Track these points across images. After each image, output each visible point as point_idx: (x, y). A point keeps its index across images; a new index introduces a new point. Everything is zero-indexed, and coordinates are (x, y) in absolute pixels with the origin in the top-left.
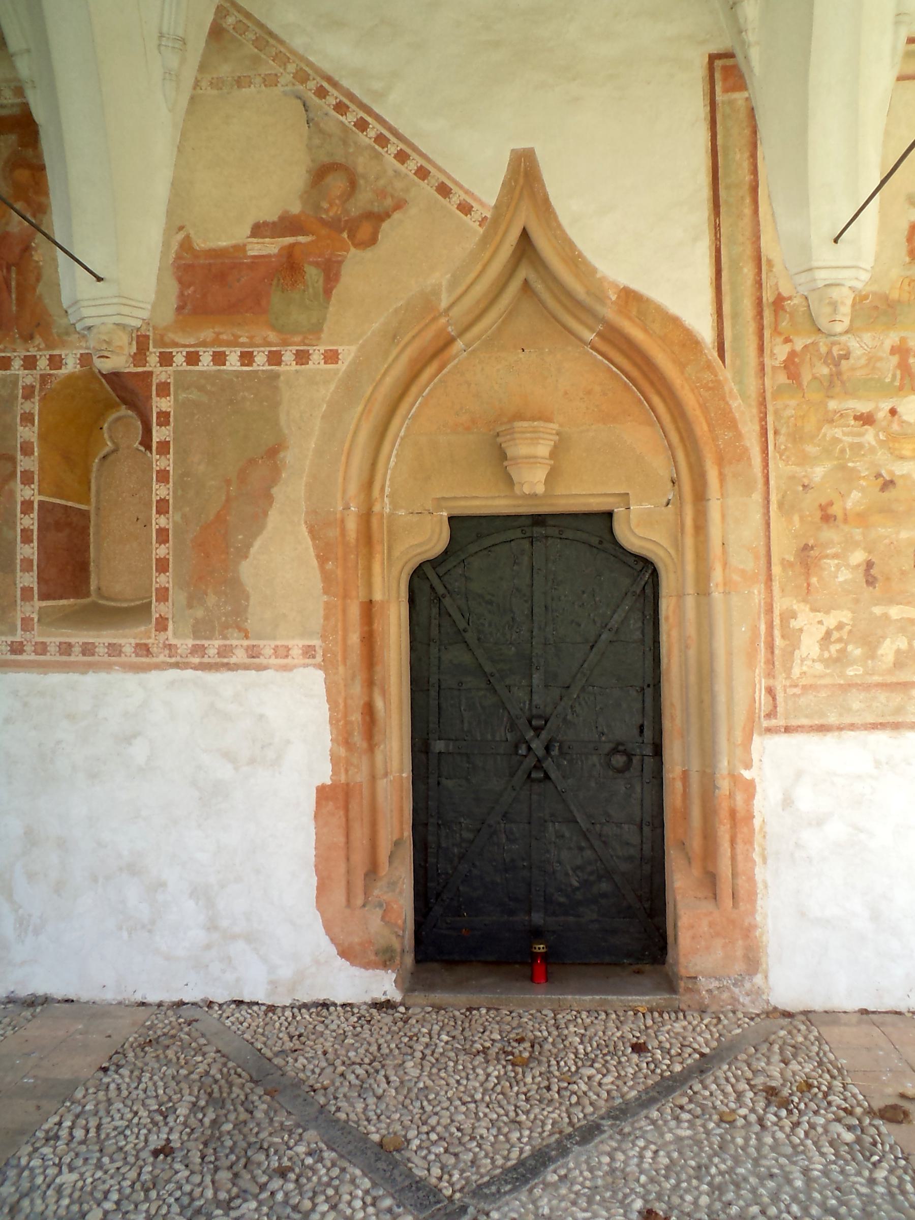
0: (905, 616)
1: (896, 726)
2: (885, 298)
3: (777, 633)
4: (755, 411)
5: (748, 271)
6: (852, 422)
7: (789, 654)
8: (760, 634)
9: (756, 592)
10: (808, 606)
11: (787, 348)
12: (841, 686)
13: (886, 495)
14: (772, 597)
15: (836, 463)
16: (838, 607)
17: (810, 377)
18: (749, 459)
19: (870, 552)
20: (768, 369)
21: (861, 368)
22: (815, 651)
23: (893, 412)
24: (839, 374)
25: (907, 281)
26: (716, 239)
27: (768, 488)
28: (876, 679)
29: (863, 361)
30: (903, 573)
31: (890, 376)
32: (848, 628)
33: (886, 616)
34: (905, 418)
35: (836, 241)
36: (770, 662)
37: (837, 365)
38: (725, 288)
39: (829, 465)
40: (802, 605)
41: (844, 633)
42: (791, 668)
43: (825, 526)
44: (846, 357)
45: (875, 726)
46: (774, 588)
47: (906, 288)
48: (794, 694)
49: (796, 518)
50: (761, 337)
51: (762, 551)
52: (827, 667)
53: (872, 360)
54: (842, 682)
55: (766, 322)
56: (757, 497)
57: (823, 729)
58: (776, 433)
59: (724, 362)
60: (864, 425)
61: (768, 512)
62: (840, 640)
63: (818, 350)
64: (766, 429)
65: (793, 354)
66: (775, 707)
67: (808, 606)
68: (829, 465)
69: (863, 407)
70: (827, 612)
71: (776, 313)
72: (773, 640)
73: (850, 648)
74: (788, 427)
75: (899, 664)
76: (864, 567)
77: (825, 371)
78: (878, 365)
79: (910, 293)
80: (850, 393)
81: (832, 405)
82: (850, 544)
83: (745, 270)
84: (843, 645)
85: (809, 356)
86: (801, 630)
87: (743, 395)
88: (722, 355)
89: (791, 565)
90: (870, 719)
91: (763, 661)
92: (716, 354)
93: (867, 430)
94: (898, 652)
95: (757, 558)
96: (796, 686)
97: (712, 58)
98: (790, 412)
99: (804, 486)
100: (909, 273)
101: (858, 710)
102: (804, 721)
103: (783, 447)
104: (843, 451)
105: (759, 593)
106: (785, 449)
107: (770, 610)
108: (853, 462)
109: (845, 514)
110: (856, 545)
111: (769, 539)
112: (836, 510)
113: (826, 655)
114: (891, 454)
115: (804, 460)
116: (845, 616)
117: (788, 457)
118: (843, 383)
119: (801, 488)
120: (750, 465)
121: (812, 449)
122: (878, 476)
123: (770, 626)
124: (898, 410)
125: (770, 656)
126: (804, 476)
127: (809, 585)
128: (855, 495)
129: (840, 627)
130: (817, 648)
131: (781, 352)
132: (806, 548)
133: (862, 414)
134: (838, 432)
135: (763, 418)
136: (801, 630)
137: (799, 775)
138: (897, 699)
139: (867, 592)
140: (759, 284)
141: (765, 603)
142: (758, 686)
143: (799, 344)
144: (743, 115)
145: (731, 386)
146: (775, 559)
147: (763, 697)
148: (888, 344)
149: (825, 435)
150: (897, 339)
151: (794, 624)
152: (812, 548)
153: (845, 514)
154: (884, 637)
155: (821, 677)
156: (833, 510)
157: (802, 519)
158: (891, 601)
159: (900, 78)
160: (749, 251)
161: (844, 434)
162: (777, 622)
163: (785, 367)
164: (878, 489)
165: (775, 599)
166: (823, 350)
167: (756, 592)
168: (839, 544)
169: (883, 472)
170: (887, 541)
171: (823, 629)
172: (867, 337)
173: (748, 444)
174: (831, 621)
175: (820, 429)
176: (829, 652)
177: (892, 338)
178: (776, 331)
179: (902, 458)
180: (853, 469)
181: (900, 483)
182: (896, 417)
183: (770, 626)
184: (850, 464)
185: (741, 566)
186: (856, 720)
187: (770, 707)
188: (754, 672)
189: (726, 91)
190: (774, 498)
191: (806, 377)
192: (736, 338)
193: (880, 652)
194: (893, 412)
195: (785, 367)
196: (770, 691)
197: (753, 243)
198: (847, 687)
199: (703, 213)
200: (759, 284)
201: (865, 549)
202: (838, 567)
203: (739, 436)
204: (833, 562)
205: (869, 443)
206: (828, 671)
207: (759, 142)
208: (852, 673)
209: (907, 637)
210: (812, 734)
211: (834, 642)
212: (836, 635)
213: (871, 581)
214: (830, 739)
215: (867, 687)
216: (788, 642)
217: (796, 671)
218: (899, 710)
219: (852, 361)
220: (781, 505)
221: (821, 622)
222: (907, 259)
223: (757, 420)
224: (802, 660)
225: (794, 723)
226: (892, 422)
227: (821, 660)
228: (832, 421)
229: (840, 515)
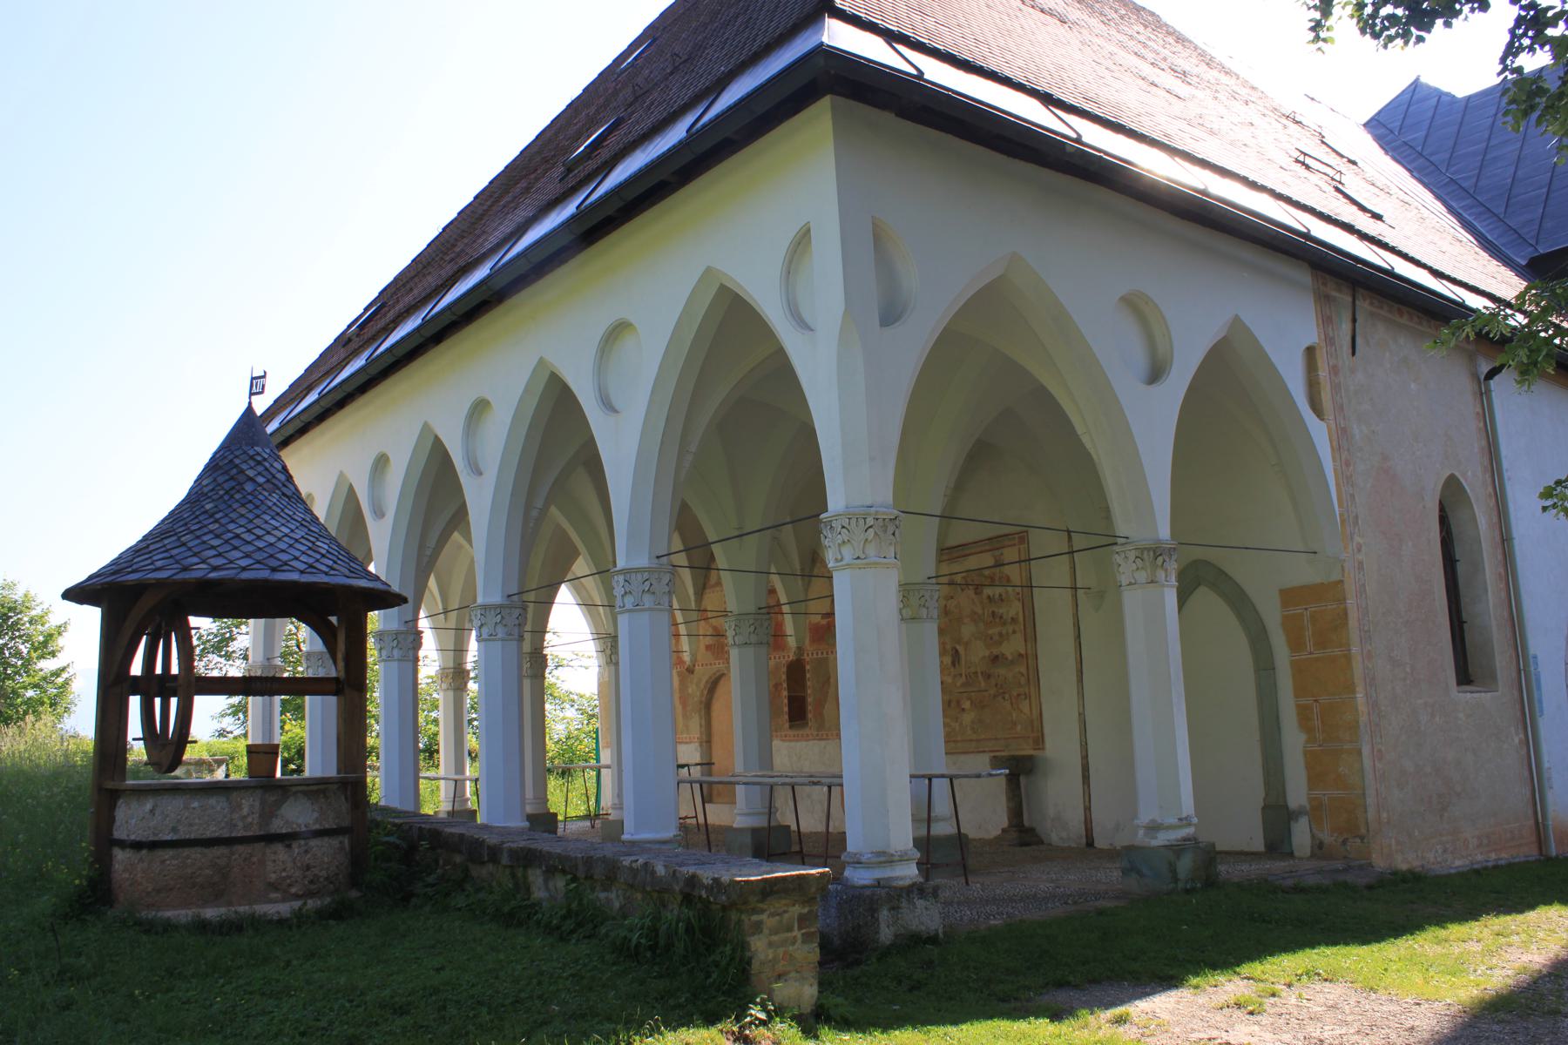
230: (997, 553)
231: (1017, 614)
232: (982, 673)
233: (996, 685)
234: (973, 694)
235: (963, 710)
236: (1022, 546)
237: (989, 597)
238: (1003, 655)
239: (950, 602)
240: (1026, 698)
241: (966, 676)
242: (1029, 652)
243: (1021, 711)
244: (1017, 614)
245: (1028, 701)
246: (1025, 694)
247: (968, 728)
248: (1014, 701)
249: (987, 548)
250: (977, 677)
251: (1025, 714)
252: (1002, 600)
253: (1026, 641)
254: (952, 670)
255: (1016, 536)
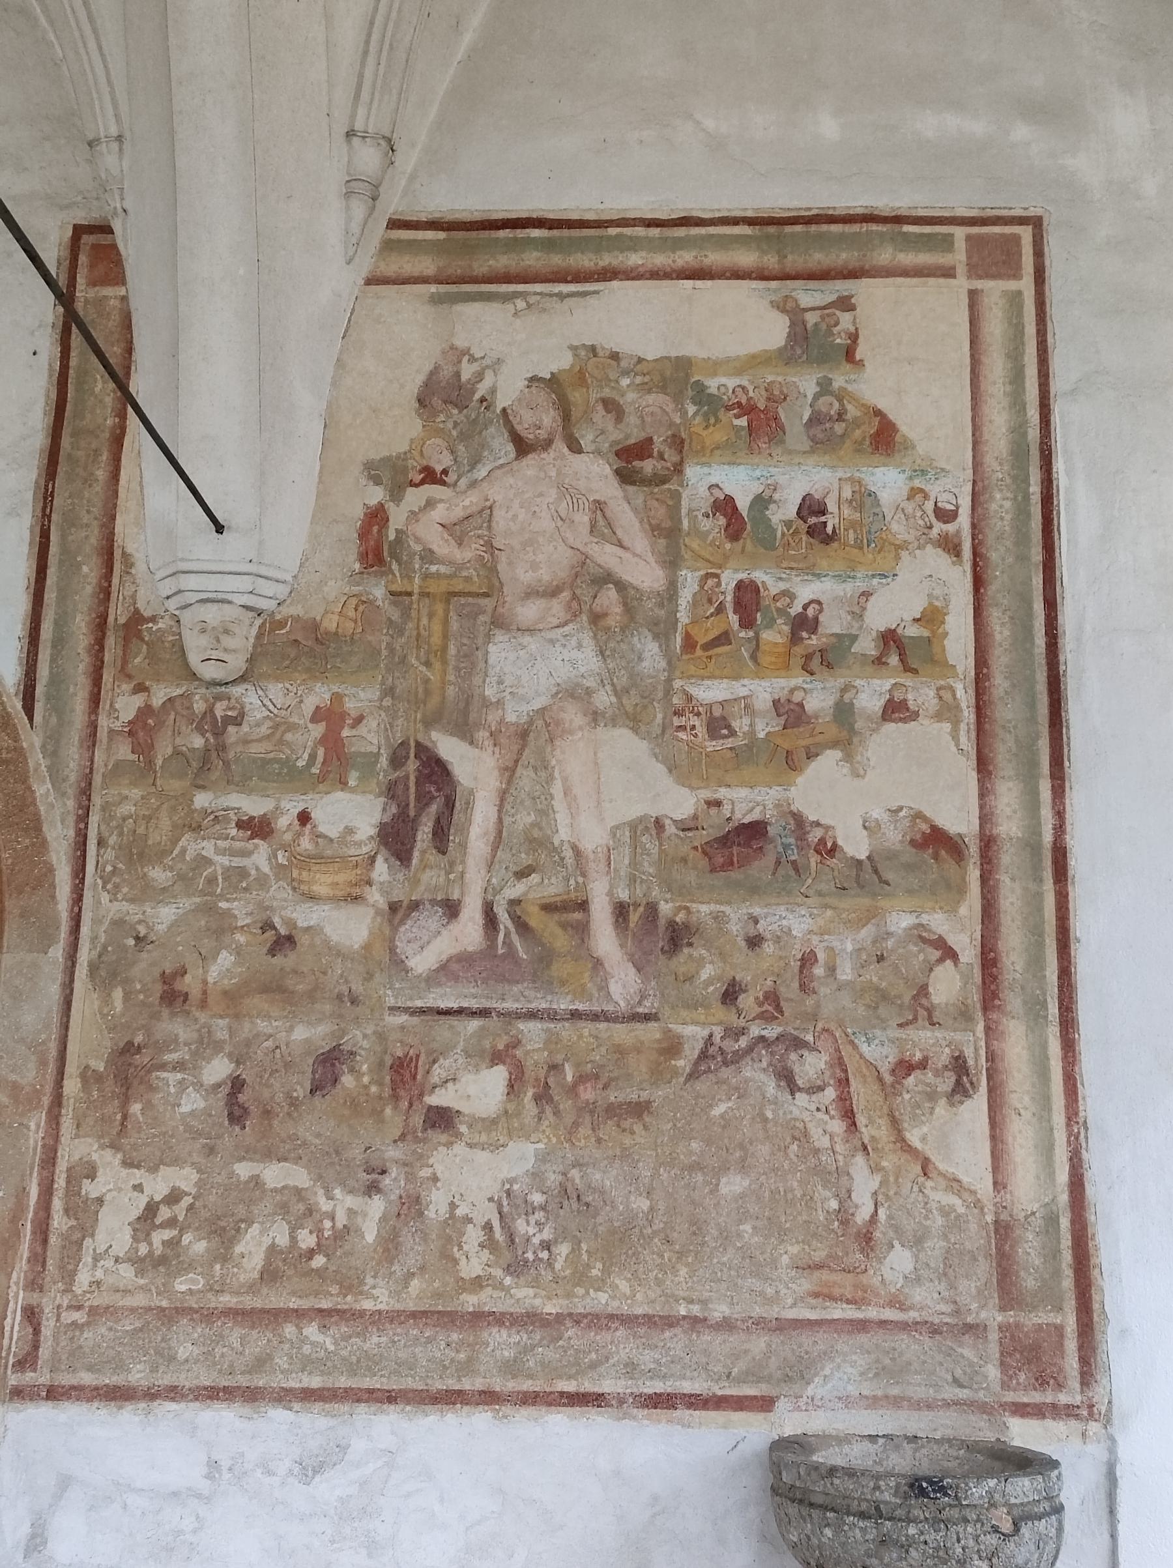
0: (291, 1183)
1: (252, 1396)
2: (313, 627)
3: (57, 1204)
4: (71, 804)
5: (90, 571)
6: (234, 832)
7: (74, 1246)
8: (28, 1205)
9: (33, 1126)
10: (119, 1156)
11: (138, 701)
12: (163, 1310)
13: (278, 960)
14: (57, 1139)
15: (198, 900)
16: (176, 1162)
17: (169, 751)
18: (53, 886)
19: (238, 1063)
20: (102, 734)
21: (259, 740)
22: (122, 1241)
23: (304, 817)
24: (222, 748)
25: (354, 601)
26: (44, 515)
27: (77, 939)
28: (227, 1300)
29: (264, 730)
30: (294, 1103)
31: (306, 756)
32: (187, 1201)
33: (256, 1181)
34: (322, 829)
35: (219, 529)
36: (38, 1259)
37: (219, 733)
38: (50, 596)
39: (187, 903)
40: (108, 1153)
41: (180, 1209)
42: (74, 1272)
43: (165, 1012)
44: (238, 721)
45: (212, 1394)
46: (63, 1119)
47: (351, 613)
48: (74, 1323)
49: (118, 994)
50: (97, 682)
51: (53, 1053)
52: (140, 1273)
53: (280, 726)
54: (165, 1304)
55: (107, 657)
56: (58, 952)
57: (118, 1395)
58: (101, 843)
59: (31, 718)
60: (252, 838)
61: (72, 981)
62: (171, 1223)
63: (190, 708)
64: (85, 836)
65: (146, 711)
66: (36, 1346)
67: (119, 1156)
68: (187, 903)
69: (253, 806)
70: (153, 1170)
71: (126, 641)
72: (48, 1216)
73: (187, 1239)
74: (121, 834)
75: (269, 1275)
76: (224, 1090)
77: (198, 742)
78: (289, 737)
79: (355, 622)
80: (242, 784)
81: (202, 800)
82: (206, 1045)
83: (85, 569)
84: (175, 1232)
85: (172, 717)
86: (100, 1201)
87: (55, 773)
88: (29, 709)
89: (99, 1078)
90: (206, 1379)
91: (26, 1255)
92: (19, 705)
93: (256, 846)
94: (272, 1249)
95: (43, 1063)
96: (79, 1308)
97: (79, 231)
98: (127, 809)
99: (138, 939)
100: (356, 589)
101: (187, 1361)
102: (87, 1378)
103: (109, 868)
104: (212, 880)
105: (38, 1126)
106: (113, 872)
107: (50, 1159)
108: (227, 900)
109: (205, 992)
110: (218, 1047)
111: (67, 1028)
112: (190, 983)
113: (143, 1249)
114: (294, 889)
115: (147, 893)
116: (185, 1178)
117: (117, 886)
118: (226, 764)
119: (132, 942)
120: (53, 897)
121: (159, 875)
122: (267, 926)
123: (47, 1191)
124: (313, 815)
125: (39, 1250)
126: (140, 922)
127: (125, 1117)
128: (225, 959)
129: (173, 1197)
130: (126, 1235)
131: (127, 706)
132: (130, 1049)
133: (252, 818)
134: (208, 848)
135: (83, 818)
136: (100, 1201)
137: (65, 1483)
138: (258, 1341)
139: (230, 1138)
140: (105, 593)
141: (44, 1146)
142: (11, 1305)
143: (160, 695)
144: (115, 319)
145: (37, 760)
146: (71, 1069)
147: (16, 1328)
148: (309, 707)
149: (184, 851)
150: (327, 696)
151: (91, 1189)
152: (139, 1049)
153: (205, 992)
154: (250, 1223)
155: (126, 1292)
156: (179, 986)
157: (127, 997)
158: (269, 1155)
159: (369, 282)
160: (94, 537)
161: (219, 851)
162: (60, 1182)
163: (130, 733)
164: (265, 950)
165: (63, 1139)
166: (199, 706)
167: (33, 1126)
168: (185, 1044)
169: (277, 921)
170: (269, 1044)
171: (143, 1201)
172: (276, 691)
173: (54, 859)
174: (158, 1186)
175: (175, 841)
176: (150, 1244)
177: (319, 695)
178: (124, 673)
179: (312, 898)
180: (228, 913)
181: (303, 940)
182: (309, 826)
183: (47, 1191)
184: (223, 905)
185: (13, 1077)
186: (184, 1380)
187: (27, 1348)
188: (9, 1276)
189: (93, 283)
190: (84, 956)
191: (163, 750)
192: (56, 681)
193: (238, 1249)
194: (304, 817)
195: (130, 733)
196: (32, 1315)
197: (103, 526)
198: (169, 1315)
199: (28, 476)
200: (105, 593)
201: (230, 1056)
202: (182, 1086)
203: (42, 845)
204: (173, 1077)
205: (257, 869)
206: (142, 1282)
207: (133, 368)
208: (183, 1288)
209: (289, 1223)
210: (96, 1404)
211: (162, 1226)
212: (164, 1213)
213: (237, 1115)
214: (129, 1416)
215: (208, 1316)
216: (73, 1222)
217: (83, 1278)
218: (261, 1363)
219: (245, 728)
220: (93, 968)
221: (138, 1188)
222: (357, 566)
223: (71, 820)
224: (96, 1259)
225: (66, 1379)
226: (299, 835)
227: (134, 1260)
228: (198, 828)
229: (195, 993)
230: (810, 296)
231: (932, 617)
232: (621, 911)
233: (731, 994)
234: (532, 1031)
235: (442, 1119)
236: (994, 290)
237: (725, 506)
238: (798, 819)
239: (414, 497)
240: (961, 1090)
241: (490, 920)
242: (1009, 826)
243: (926, 1167)
244: (932, 617)
245: (978, 1103)
246: (959, 1065)
247: (473, 1236)
248: (862, 1093)
249: (746, 258)
250: (582, 930)
251: (954, 1184)
252: (821, 535)
253: (984, 765)
254: (381, 870)
255: (960, 232)
